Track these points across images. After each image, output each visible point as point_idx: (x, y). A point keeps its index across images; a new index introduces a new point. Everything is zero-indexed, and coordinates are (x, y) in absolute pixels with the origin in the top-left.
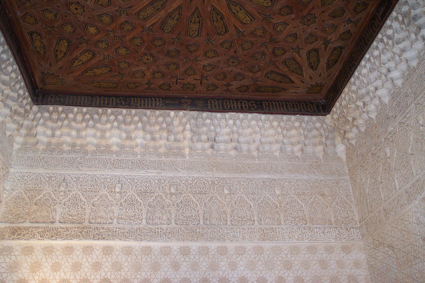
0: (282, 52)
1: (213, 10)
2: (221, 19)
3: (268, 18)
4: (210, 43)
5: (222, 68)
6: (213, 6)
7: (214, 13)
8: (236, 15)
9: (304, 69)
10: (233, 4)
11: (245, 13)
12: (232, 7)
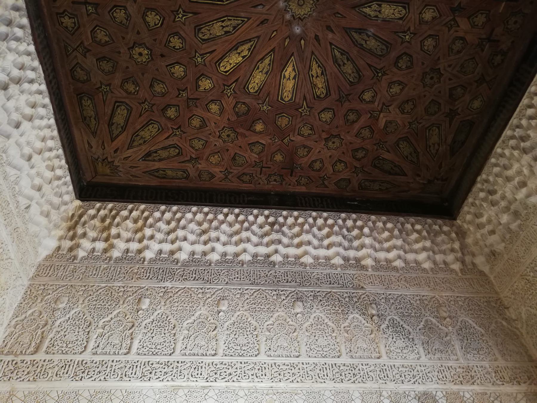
0: (172, 117)
1: (241, 20)
2: (226, 32)
3: (231, 91)
4: (179, 17)
5: (123, 38)
6: (249, 19)
7: (236, 22)
8: (235, 52)
9: (144, 147)
10: (251, 46)
11: (238, 63)
12: (247, 46)
